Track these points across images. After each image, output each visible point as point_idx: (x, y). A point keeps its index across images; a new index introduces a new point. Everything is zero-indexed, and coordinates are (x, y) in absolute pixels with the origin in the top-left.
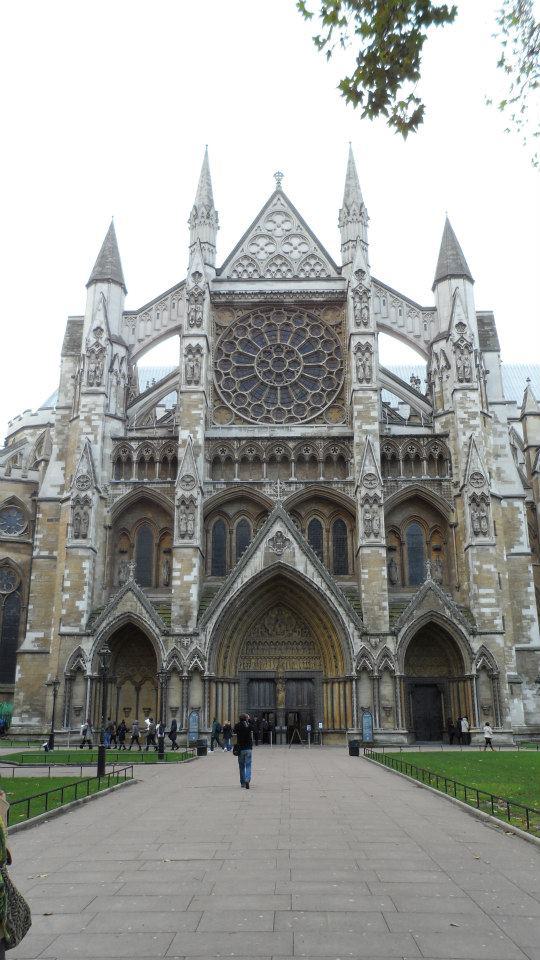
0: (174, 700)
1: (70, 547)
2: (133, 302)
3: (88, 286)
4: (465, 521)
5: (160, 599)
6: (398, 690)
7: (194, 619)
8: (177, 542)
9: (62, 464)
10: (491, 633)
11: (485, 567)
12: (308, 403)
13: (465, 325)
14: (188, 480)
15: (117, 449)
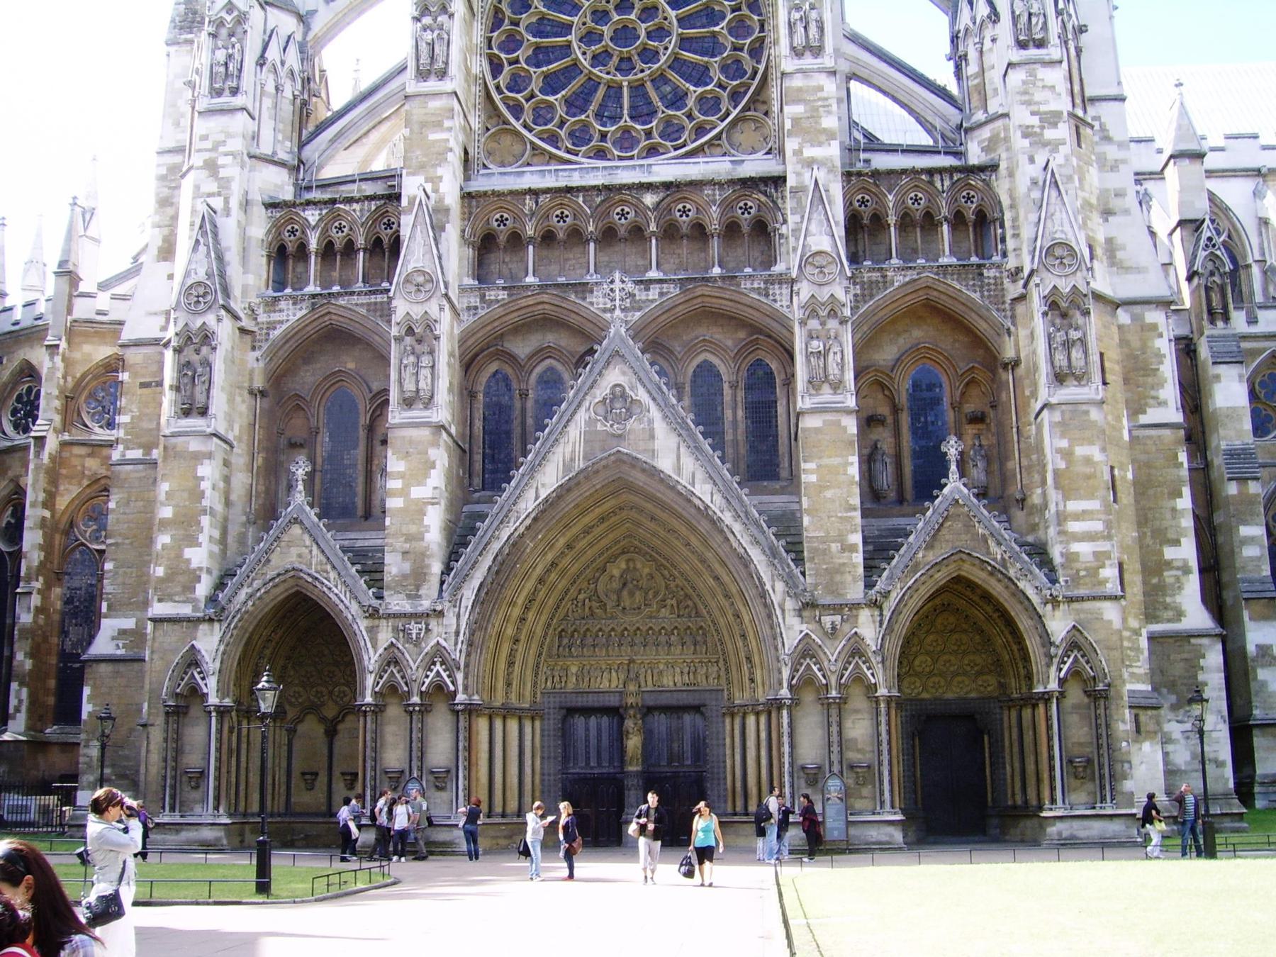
0: (394, 757)
1: (174, 435)
4: (1034, 352)
5: (367, 543)
6: (883, 728)
7: (434, 581)
8: (395, 415)
10: (1094, 598)
11: (1080, 451)
12: (690, 116)
14: (421, 279)
15: (277, 228)
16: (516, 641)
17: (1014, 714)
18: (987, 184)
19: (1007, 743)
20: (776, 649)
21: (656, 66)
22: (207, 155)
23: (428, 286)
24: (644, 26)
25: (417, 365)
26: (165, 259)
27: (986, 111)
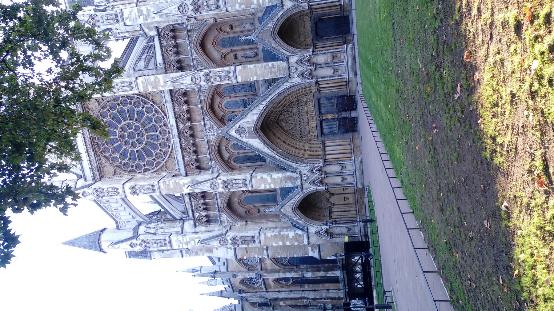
0: (338, 180)
2: (112, 225)
3: (105, 253)
6: (321, 52)
9: (214, 250)
12: (154, 115)
14: (213, 185)
15: (201, 224)
16: (305, 150)
17: (314, 11)
19: (323, 12)
21: (140, 126)
22: (184, 245)
23: (214, 183)
24: (128, 130)
25: (236, 184)
26: (212, 251)
27: (140, 30)
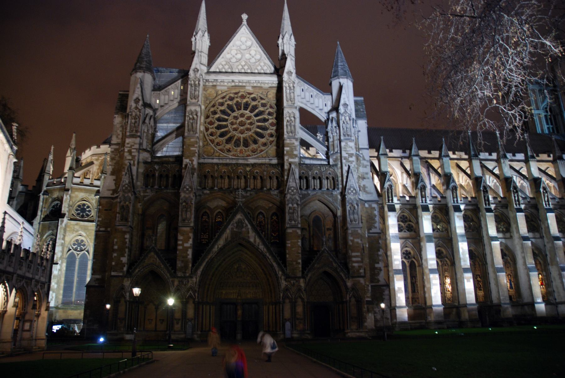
7: (190, 269)
9: (114, 177)
13: (348, 105)
18: (334, 170)
20: (279, 288)
22: (129, 149)
